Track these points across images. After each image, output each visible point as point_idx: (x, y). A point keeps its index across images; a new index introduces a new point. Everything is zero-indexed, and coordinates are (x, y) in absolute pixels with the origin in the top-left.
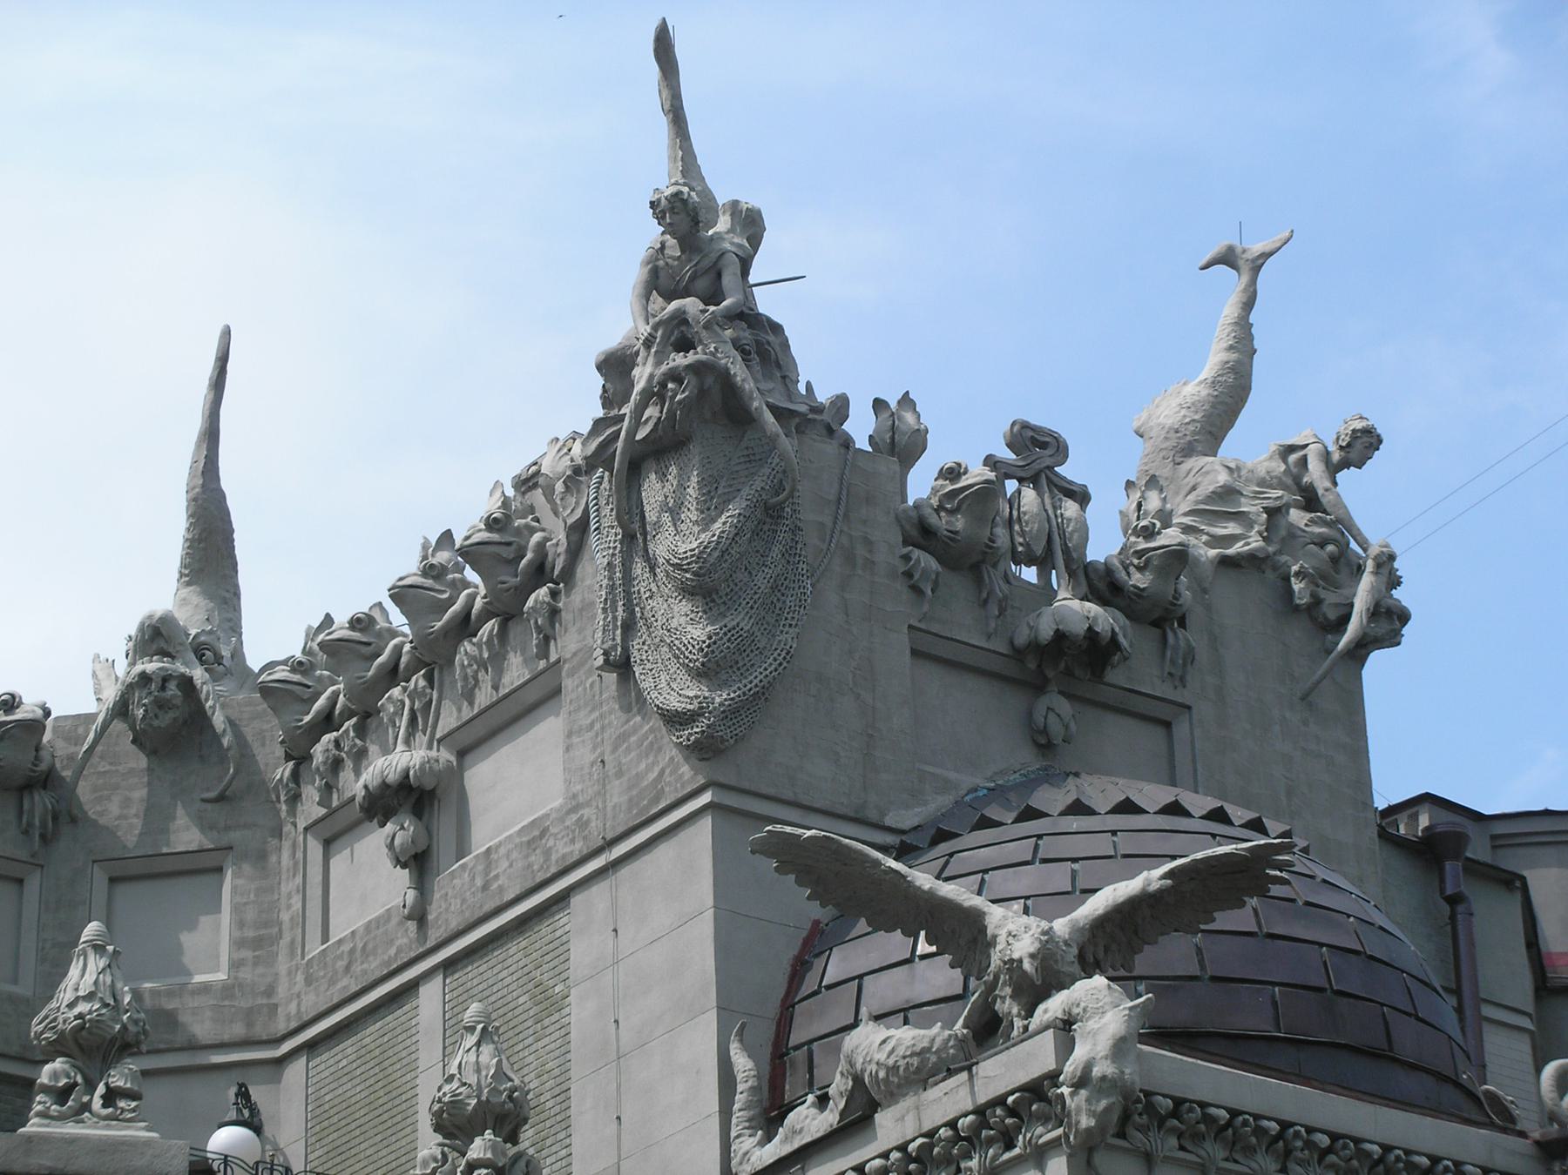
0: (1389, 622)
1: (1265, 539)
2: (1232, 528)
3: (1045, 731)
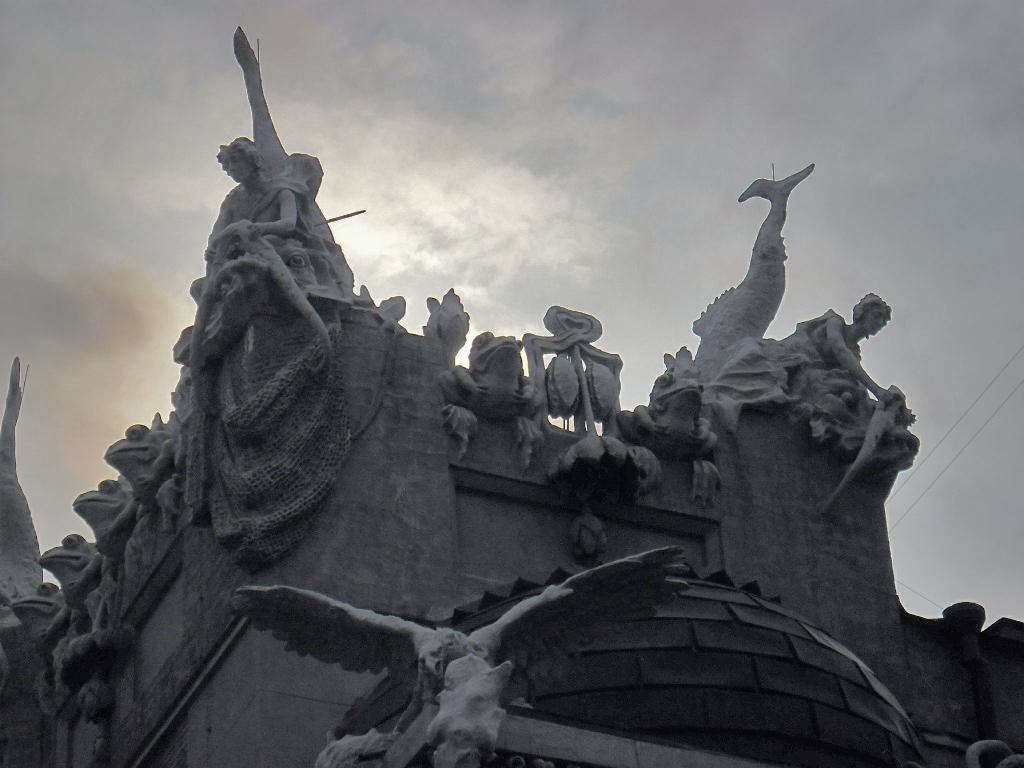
0: (898, 449)
1: (785, 391)
2: (759, 385)
3: (578, 544)
